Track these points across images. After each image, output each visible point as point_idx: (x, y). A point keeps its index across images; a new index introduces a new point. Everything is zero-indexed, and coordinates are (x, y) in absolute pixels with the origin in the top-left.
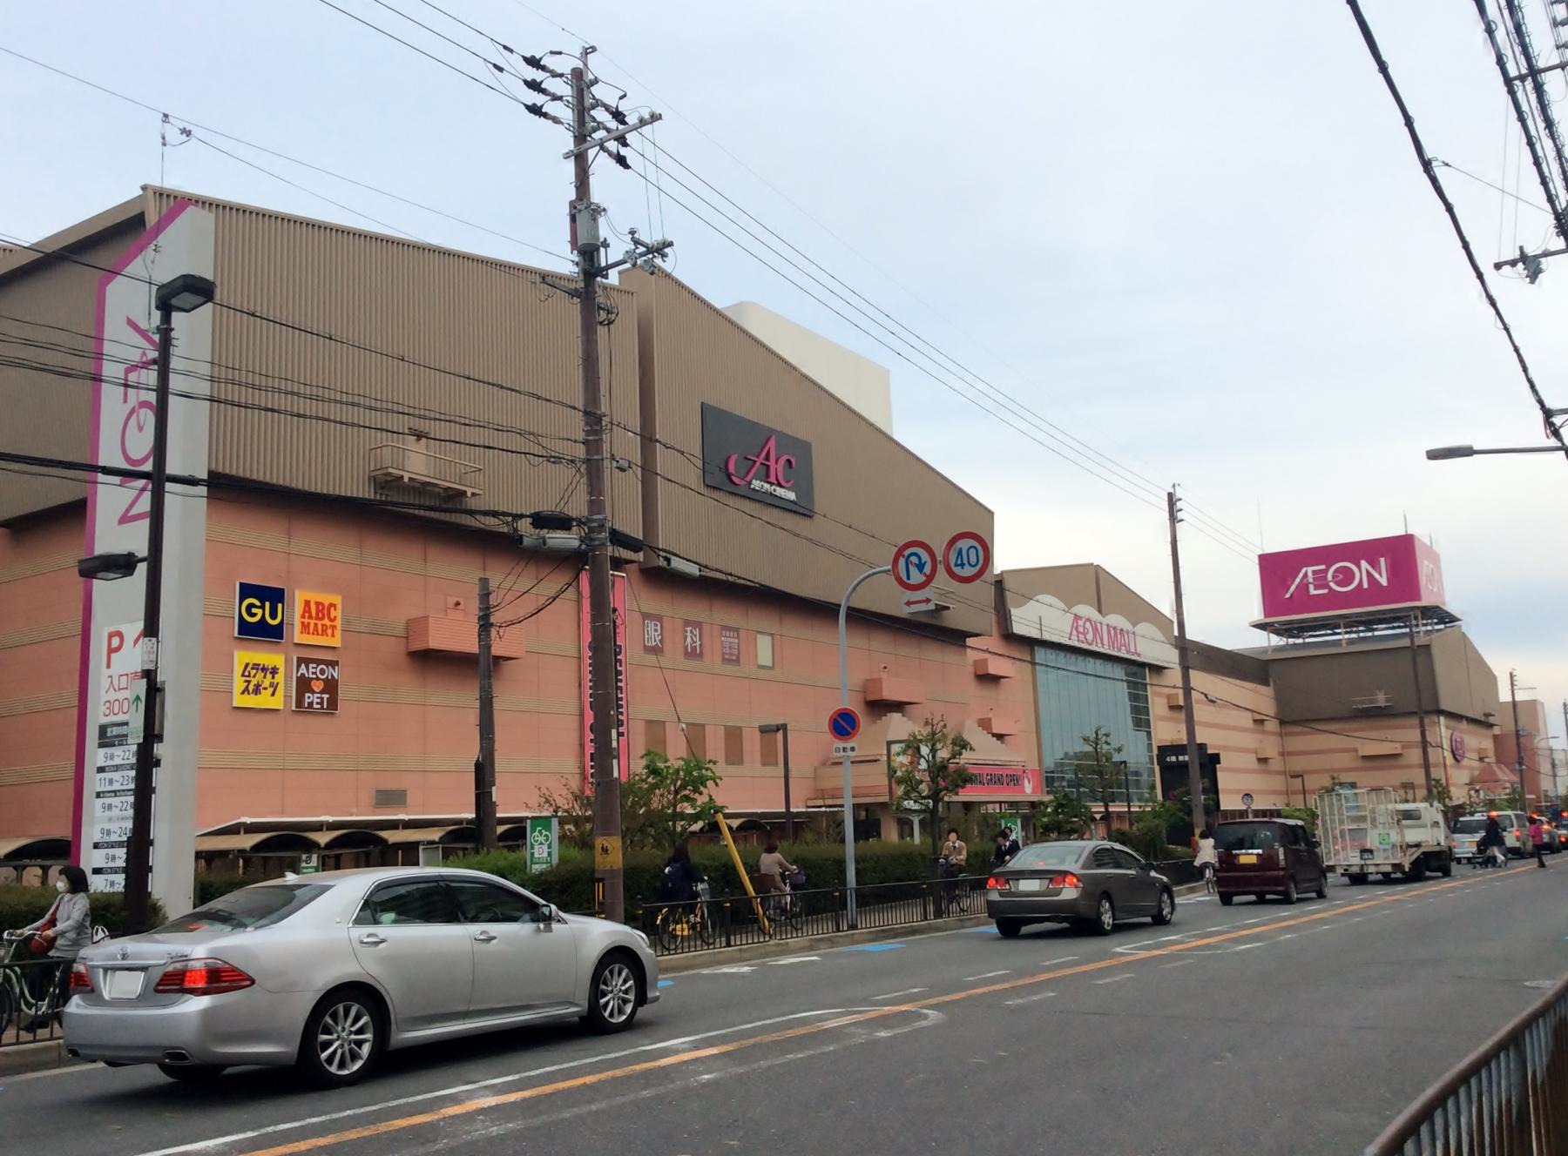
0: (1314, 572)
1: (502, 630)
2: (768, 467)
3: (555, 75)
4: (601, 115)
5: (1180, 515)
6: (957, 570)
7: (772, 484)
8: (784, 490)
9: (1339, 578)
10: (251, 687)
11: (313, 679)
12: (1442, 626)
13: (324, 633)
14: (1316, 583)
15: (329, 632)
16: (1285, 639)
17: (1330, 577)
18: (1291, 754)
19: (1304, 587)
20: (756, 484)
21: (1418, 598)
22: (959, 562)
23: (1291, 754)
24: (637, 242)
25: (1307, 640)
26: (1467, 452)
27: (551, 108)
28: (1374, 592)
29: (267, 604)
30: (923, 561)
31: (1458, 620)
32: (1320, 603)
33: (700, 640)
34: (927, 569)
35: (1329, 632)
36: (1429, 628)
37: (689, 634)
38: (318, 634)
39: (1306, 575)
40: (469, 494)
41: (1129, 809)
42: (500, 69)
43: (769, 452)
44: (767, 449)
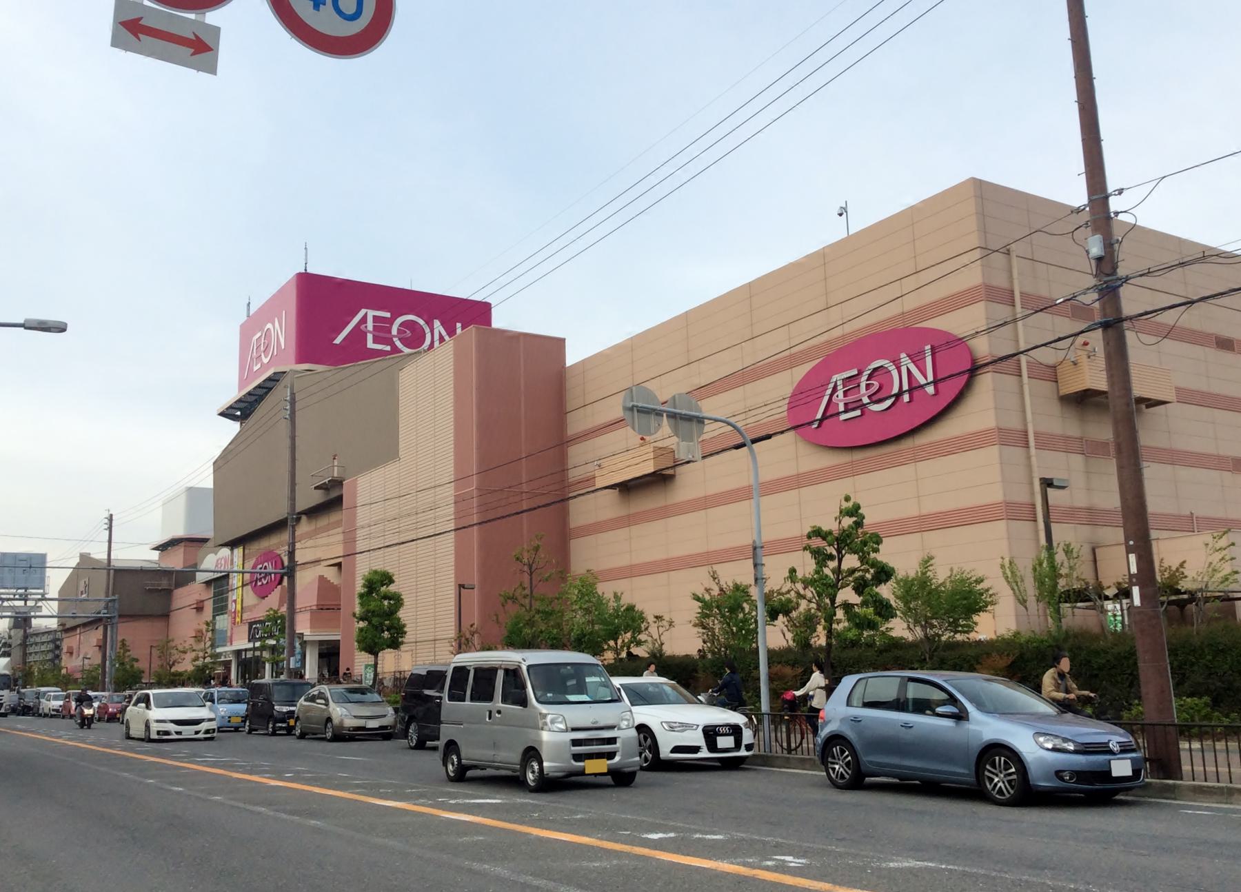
0: (375, 318)
14: (377, 334)
17: (394, 331)
19: (358, 333)
39: (364, 320)
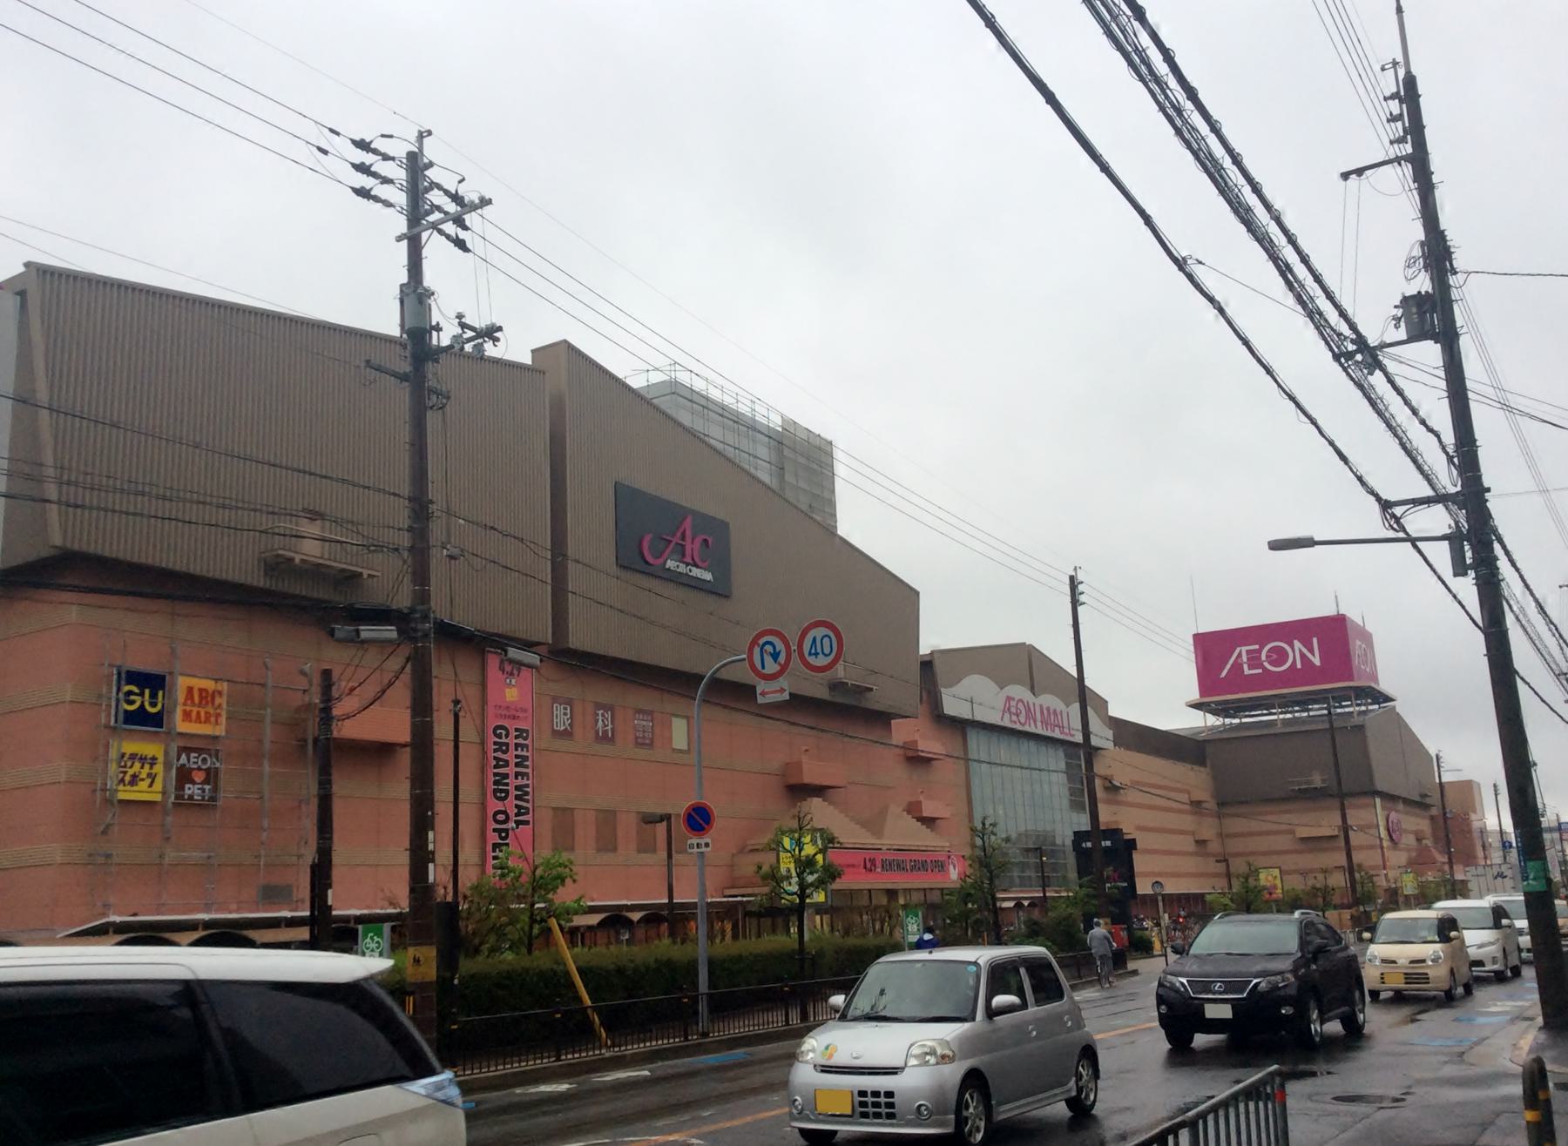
0: (1248, 652)
1: (340, 723)
2: (683, 546)
3: (386, 157)
4: (436, 197)
5: (1082, 598)
6: (812, 660)
7: (687, 564)
8: (699, 570)
10: (127, 778)
11: (194, 769)
12: (1377, 706)
13: (207, 721)
15: (213, 719)
16: (1221, 719)
17: (1263, 657)
18: (1228, 836)
19: (1237, 666)
20: (671, 564)
21: (1351, 678)
22: (813, 651)
23: (1228, 836)
24: (463, 326)
25: (1244, 720)
26: (1308, 543)
27: (381, 191)
28: (1307, 672)
29: (147, 692)
30: (777, 650)
31: (1392, 700)
32: (1254, 684)
33: (612, 723)
34: (782, 658)
35: (1265, 712)
36: (1363, 708)
37: (600, 718)
38: (200, 722)
39: (1240, 655)
40: (365, 576)
41: (1044, 894)
42: (325, 152)
43: (684, 531)
44: (681, 530)
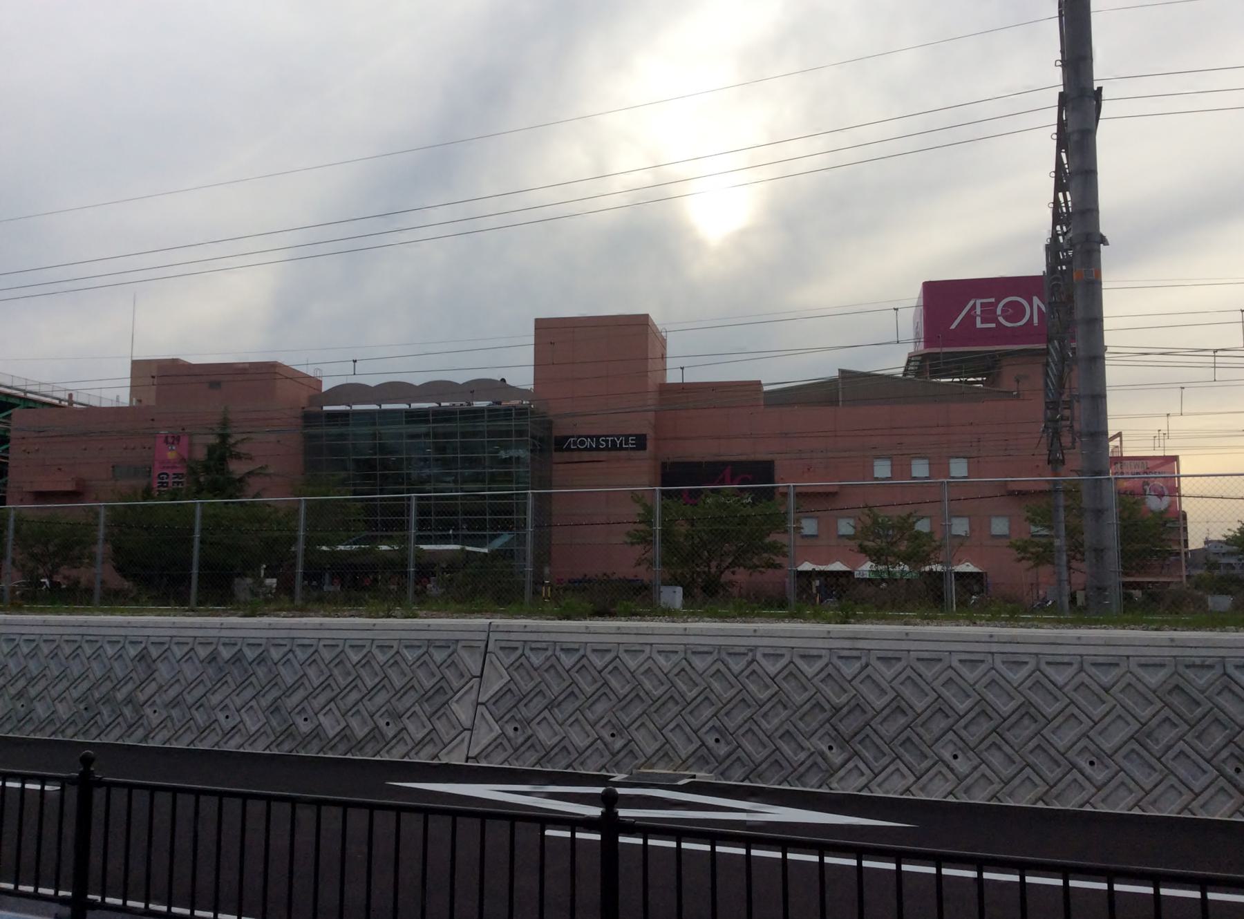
9: (1009, 313)
17: (999, 312)
19: (970, 317)
32: (986, 336)
39: (974, 306)
